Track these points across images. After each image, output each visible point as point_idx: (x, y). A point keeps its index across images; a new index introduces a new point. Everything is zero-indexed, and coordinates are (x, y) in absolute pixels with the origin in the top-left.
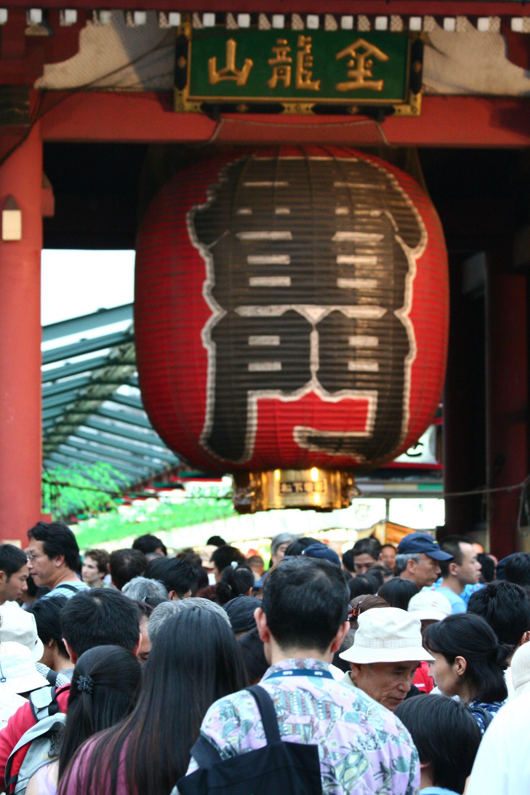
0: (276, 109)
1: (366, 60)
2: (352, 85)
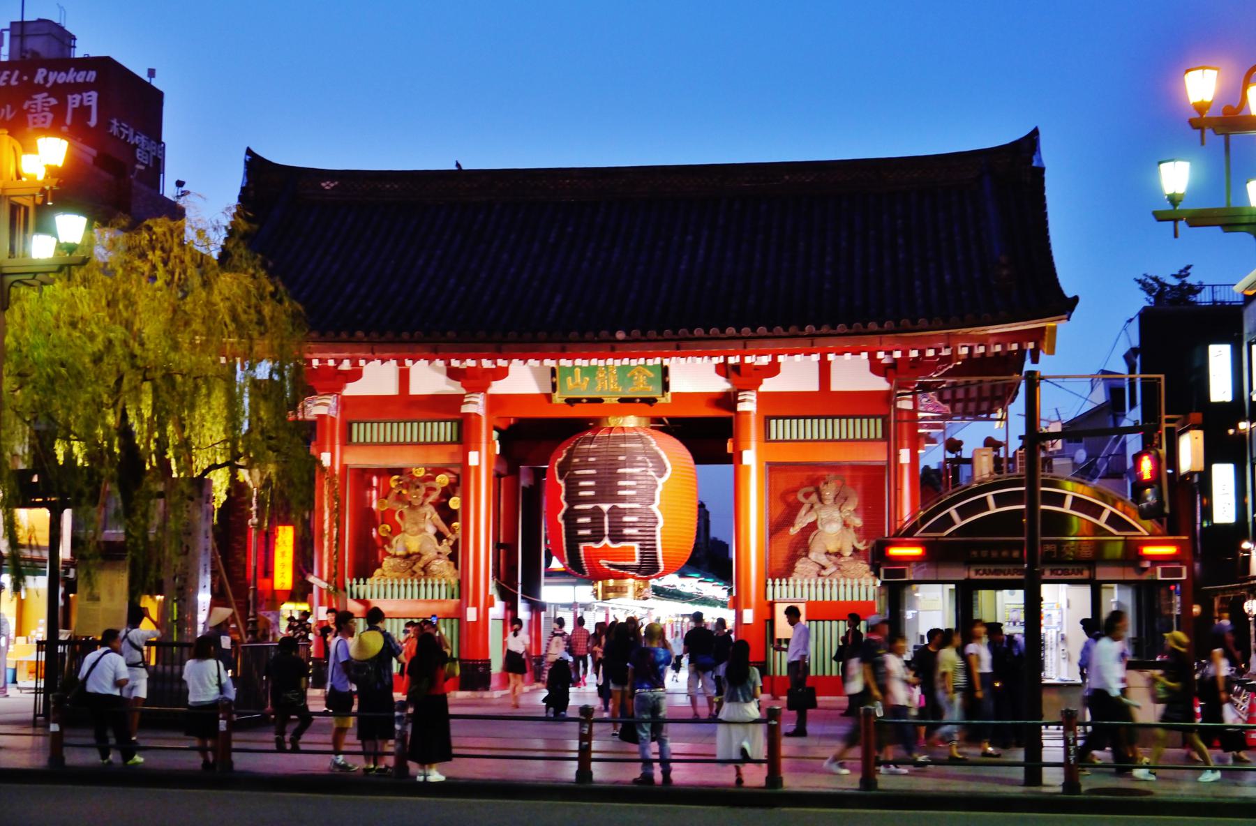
0: (600, 400)
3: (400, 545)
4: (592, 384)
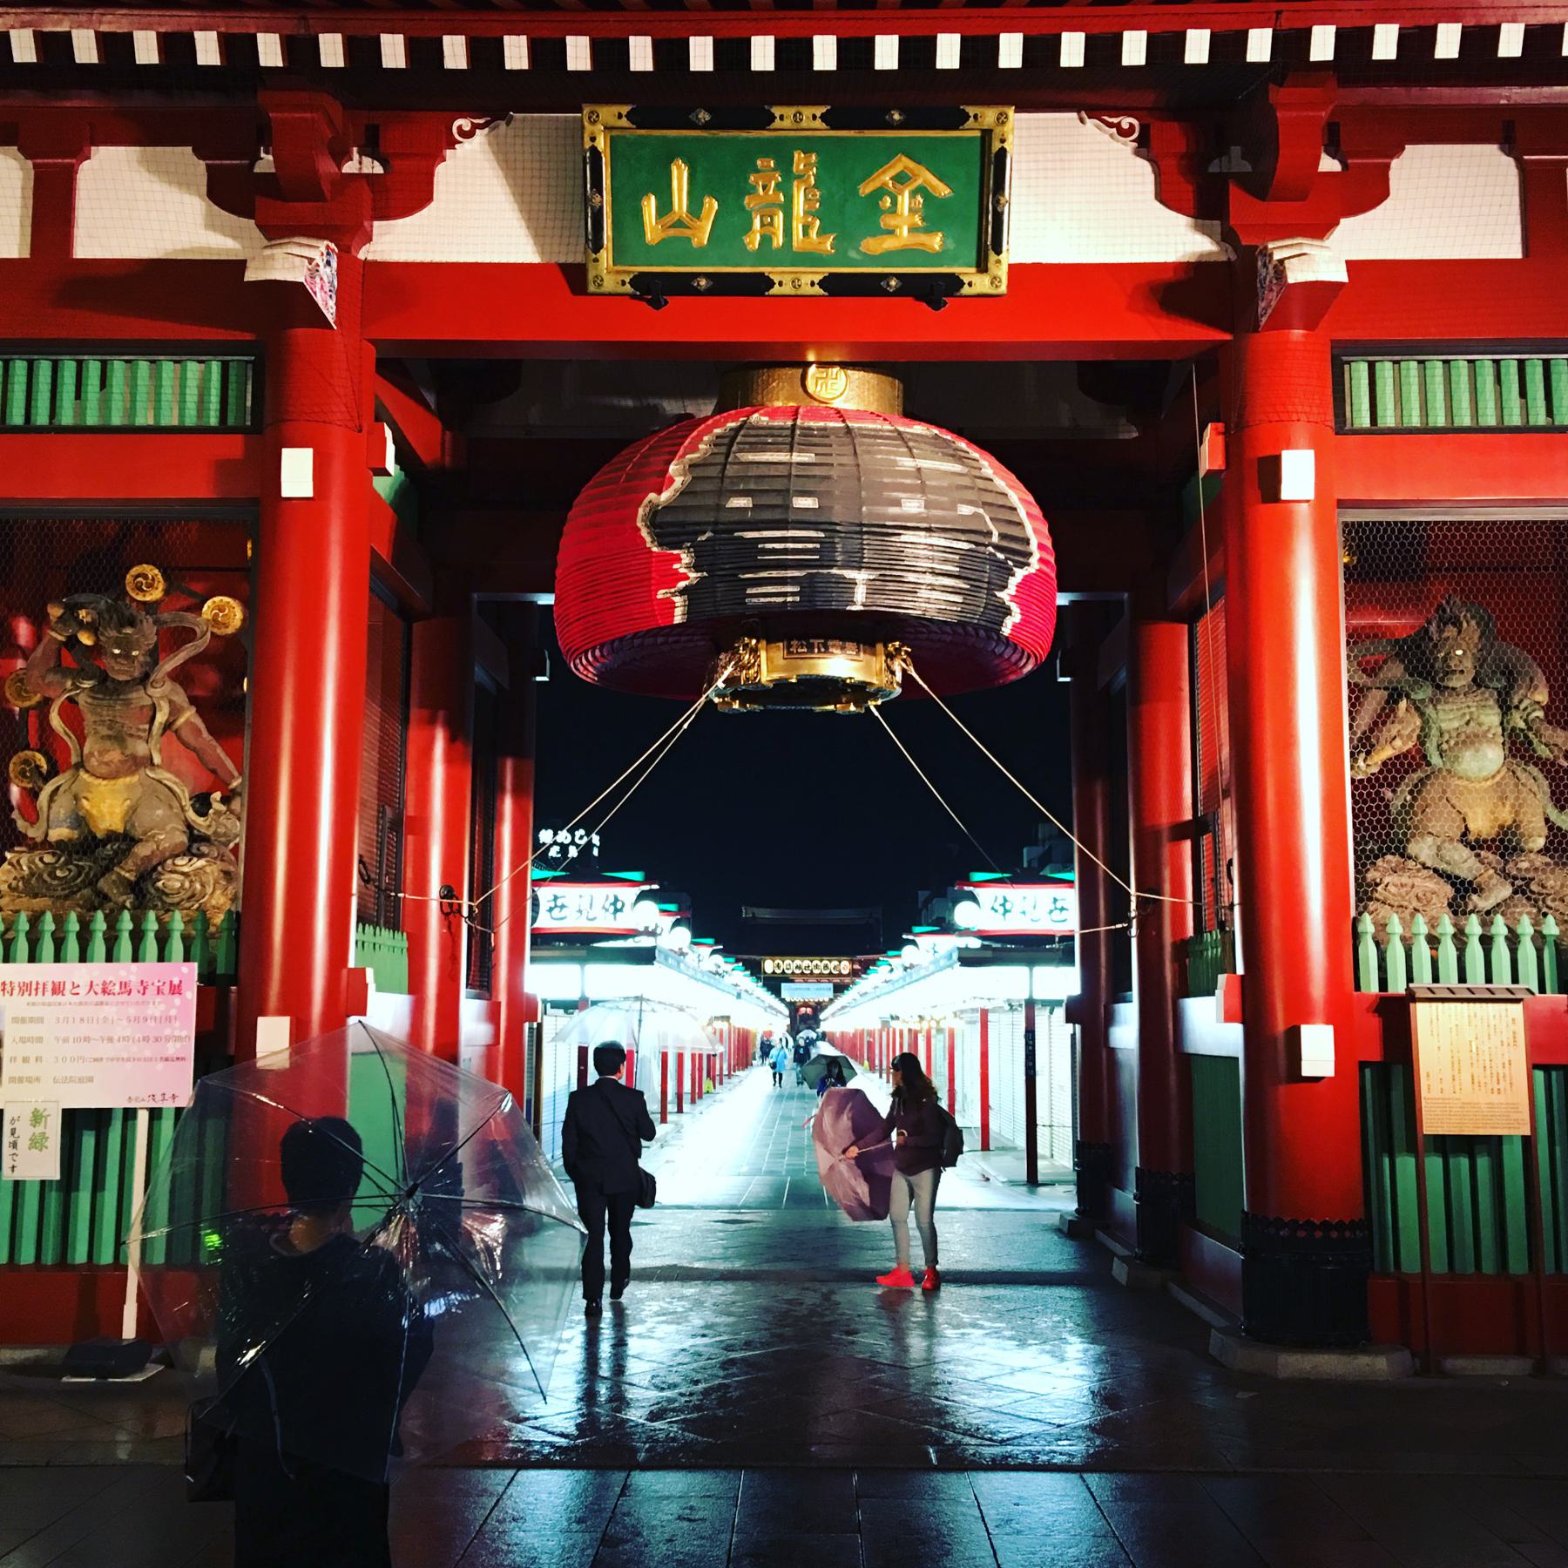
0: (759, 284)
1: (913, 194)
2: (889, 244)
3: (62, 808)
4: (732, 224)
